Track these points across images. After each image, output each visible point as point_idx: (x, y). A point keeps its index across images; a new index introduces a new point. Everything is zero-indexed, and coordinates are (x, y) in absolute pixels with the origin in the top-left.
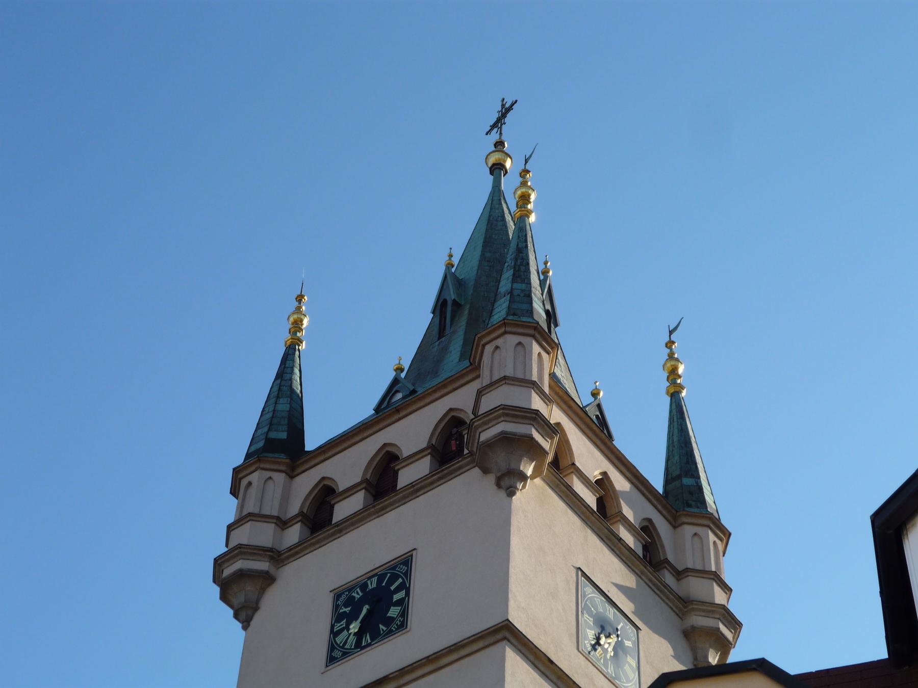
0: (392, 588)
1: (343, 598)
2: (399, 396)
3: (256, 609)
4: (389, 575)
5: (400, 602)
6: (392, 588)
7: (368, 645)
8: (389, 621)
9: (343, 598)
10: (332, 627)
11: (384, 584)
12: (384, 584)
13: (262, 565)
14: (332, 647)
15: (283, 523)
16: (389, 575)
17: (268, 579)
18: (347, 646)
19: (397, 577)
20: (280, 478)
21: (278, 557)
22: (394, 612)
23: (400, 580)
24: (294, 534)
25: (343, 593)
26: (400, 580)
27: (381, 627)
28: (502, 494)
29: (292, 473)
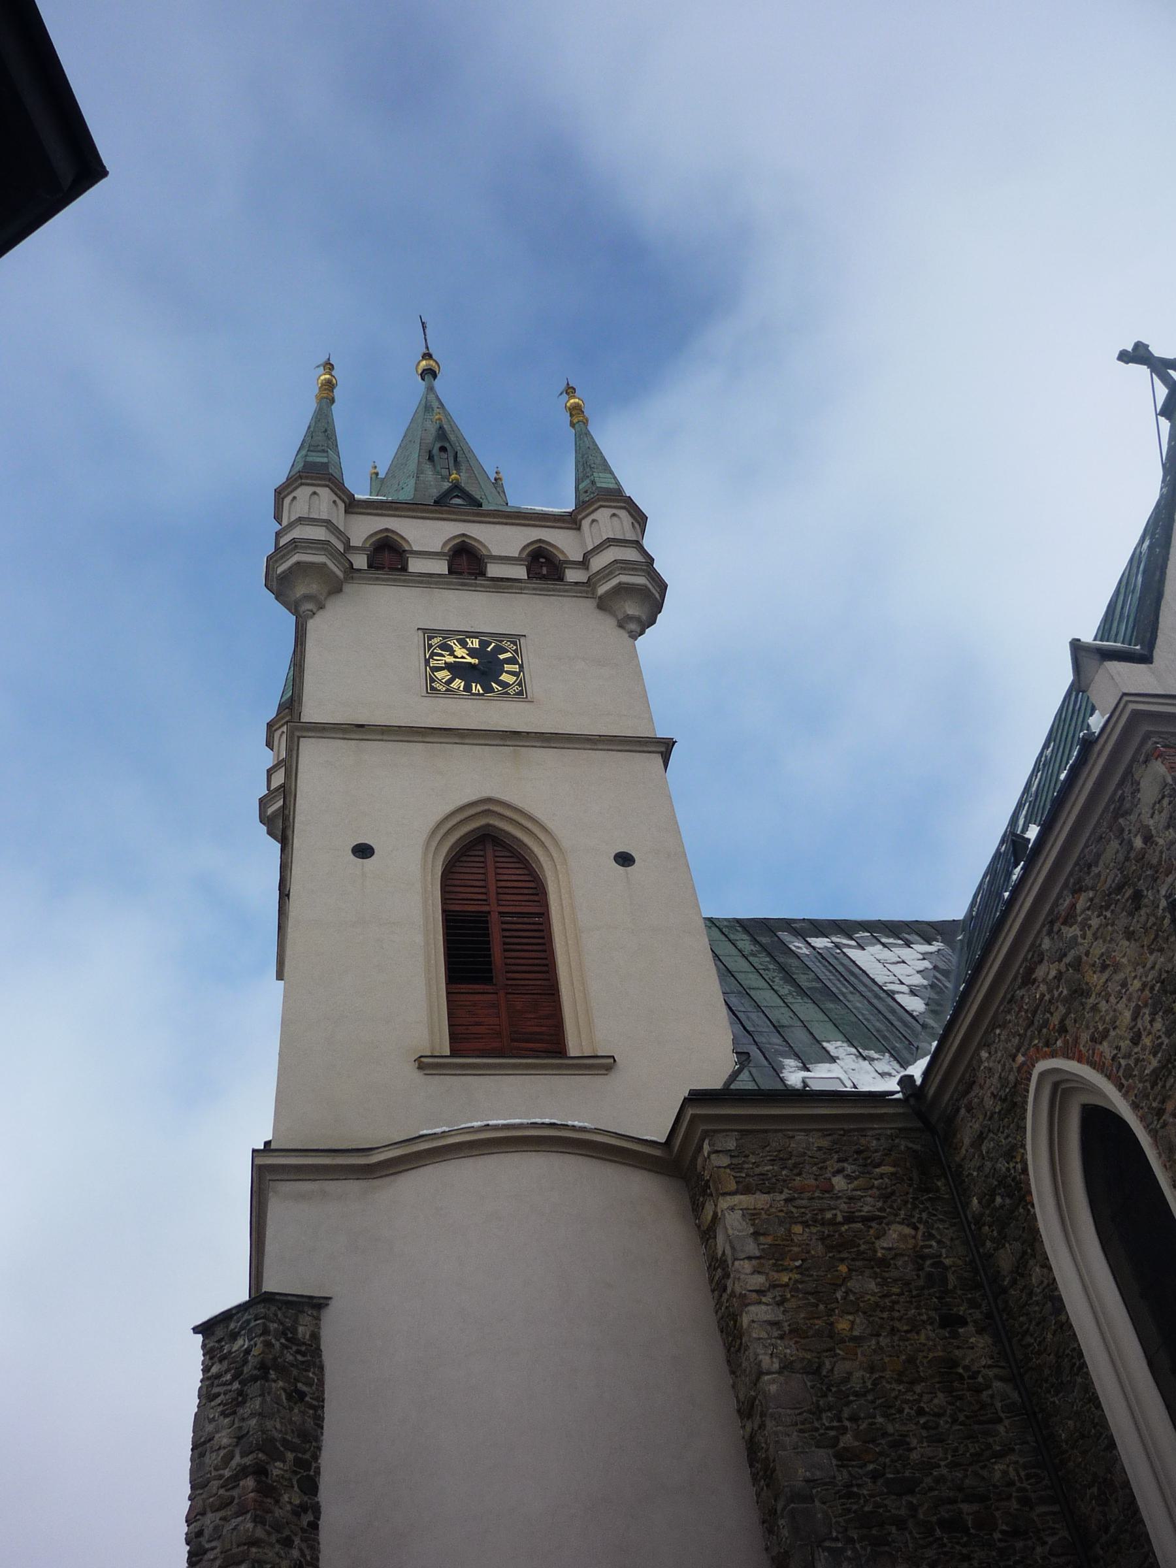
0: (502, 657)
3: (321, 607)
4: (493, 644)
6: (502, 657)
7: (482, 695)
8: (505, 685)
9: (434, 641)
10: (427, 662)
11: (489, 649)
12: (489, 649)
16: (493, 644)
23: (508, 655)
24: (360, 561)
25: (436, 637)
27: (494, 685)
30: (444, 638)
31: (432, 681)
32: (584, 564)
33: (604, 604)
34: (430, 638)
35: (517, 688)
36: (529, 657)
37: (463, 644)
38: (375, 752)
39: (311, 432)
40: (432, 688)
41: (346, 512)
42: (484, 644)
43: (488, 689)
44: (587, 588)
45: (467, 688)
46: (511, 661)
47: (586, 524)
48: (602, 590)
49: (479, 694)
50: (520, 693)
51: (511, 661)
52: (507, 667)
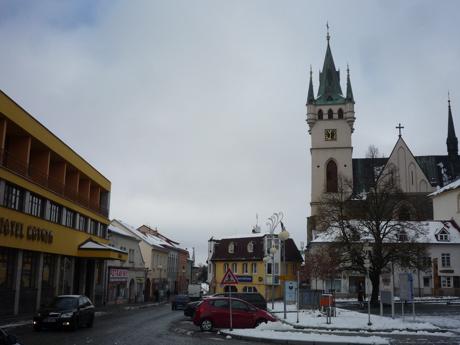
0: (334, 133)
1: (326, 131)
3: (313, 127)
5: (335, 136)
6: (334, 133)
8: (334, 138)
9: (326, 131)
14: (326, 138)
17: (314, 123)
20: (314, 106)
21: (316, 120)
22: (334, 137)
23: (335, 133)
24: (317, 117)
26: (335, 133)
29: (316, 105)
33: (347, 122)
34: (326, 131)
35: (335, 139)
36: (337, 133)
37: (329, 131)
38: (319, 150)
39: (309, 97)
40: (326, 140)
42: (332, 131)
43: (332, 139)
46: (335, 134)
47: (346, 105)
48: (348, 120)
51: (335, 134)
52: (335, 135)
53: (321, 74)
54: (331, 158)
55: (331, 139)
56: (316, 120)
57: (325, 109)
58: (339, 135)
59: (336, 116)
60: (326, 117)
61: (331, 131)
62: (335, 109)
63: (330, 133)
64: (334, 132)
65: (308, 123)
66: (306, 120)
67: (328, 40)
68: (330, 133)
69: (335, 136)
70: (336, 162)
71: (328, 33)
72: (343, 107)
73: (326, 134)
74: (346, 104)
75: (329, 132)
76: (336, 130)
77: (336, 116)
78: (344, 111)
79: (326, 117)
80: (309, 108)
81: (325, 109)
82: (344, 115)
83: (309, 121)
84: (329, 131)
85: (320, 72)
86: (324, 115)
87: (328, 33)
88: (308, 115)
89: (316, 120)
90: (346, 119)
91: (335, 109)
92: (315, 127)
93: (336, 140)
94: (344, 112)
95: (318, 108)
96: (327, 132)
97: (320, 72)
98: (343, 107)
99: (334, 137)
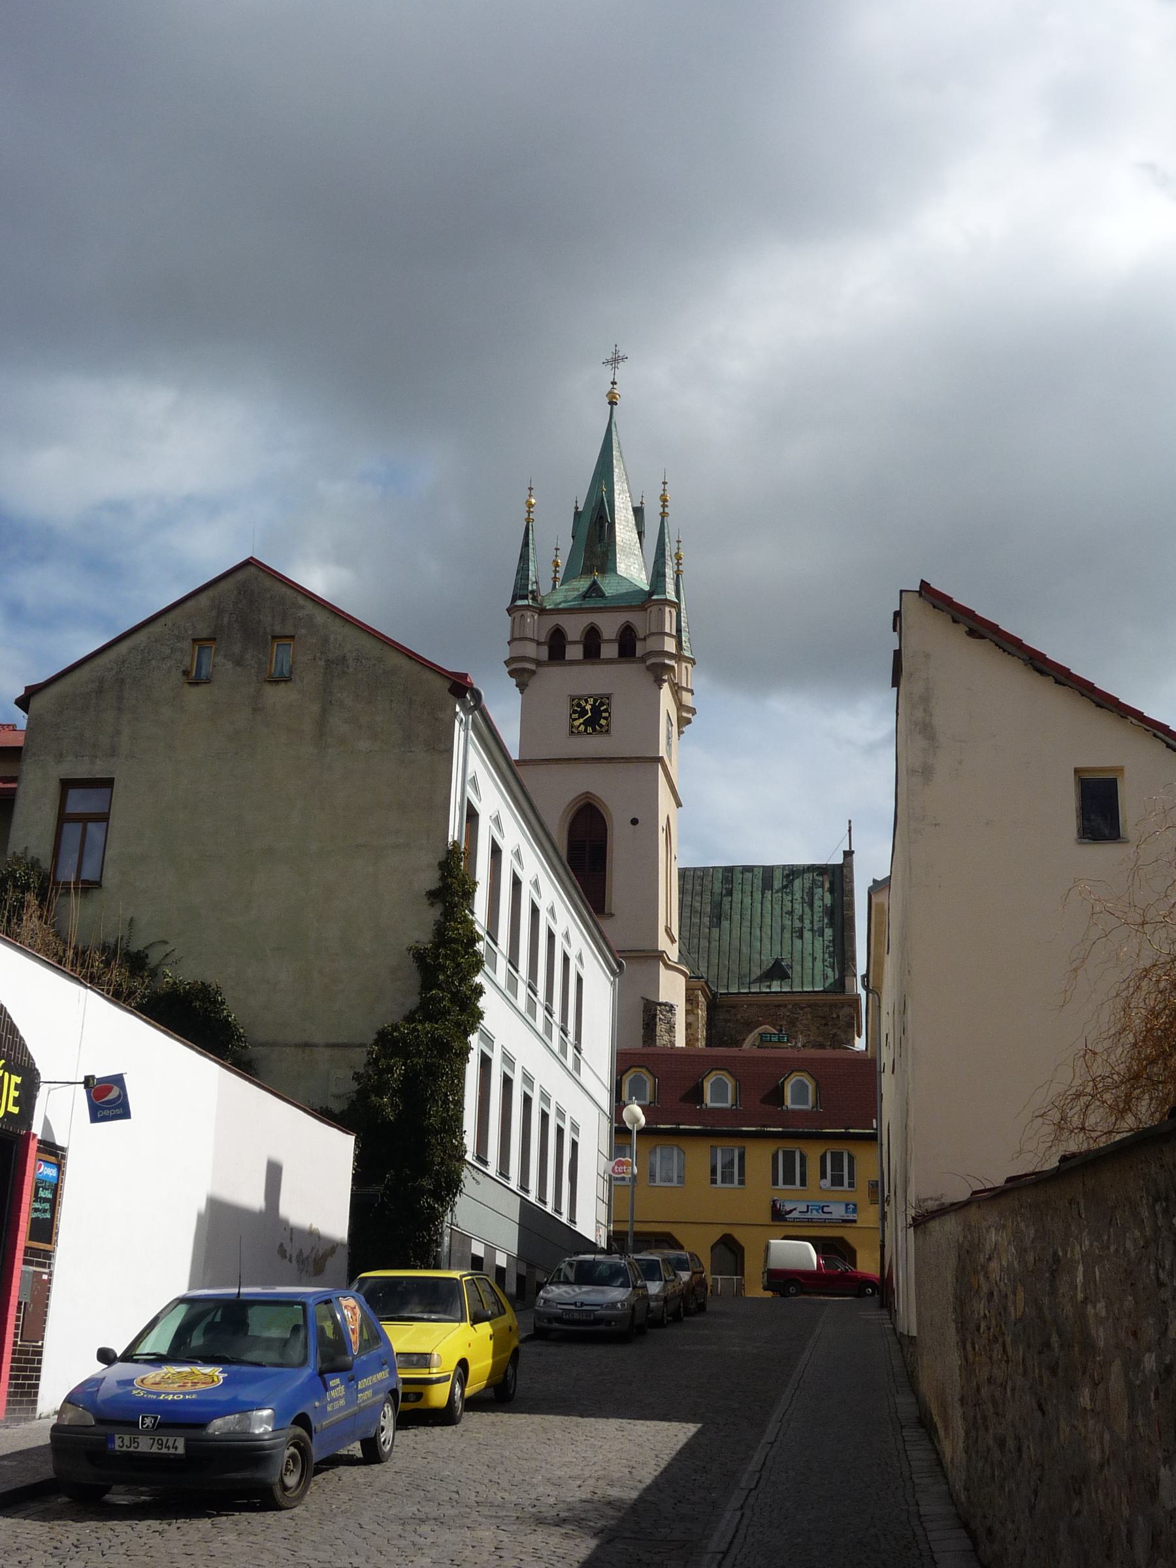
0: (602, 709)
2: (594, 595)
5: (606, 718)
6: (602, 709)
7: (590, 734)
8: (601, 726)
10: (571, 715)
13: (532, 667)
15: (539, 643)
17: (533, 672)
18: (580, 729)
19: (604, 705)
23: (605, 707)
24: (544, 653)
26: (605, 707)
28: (656, 687)
30: (579, 699)
31: (572, 727)
32: (644, 639)
33: (648, 668)
34: (573, 700)
36: (614, 709)
37: (587, 702)
40: (572, 732)
41: (539, 615)
42: (595, 701)
43: (594, 730)
44: (643, 660)
45: (586, 730)
46: (606, 711)
47: (649, 610)
48: (649, 662)
49: (590, 734)
50: (607, 731)
51: (606, 711)
52: (604, 715)
53: (577, 515)
54: (588, 793)
55: (590, 730)
56: (540, 662)
57: (574, 628)
58: (619, 715)
59: (609, 651)
60: (574, 652)
61: (591, 701)
62: (610, 626)
63: (588, 707)
64: (602, 704)
65: (512, 673)
66: (507, 663)
67: (612, 403)
68: (588, 707)
69: (606, 718)
70: (595, 801)
71: (614, 383)
72: (635, 618)
73: (575, 712)
74: (646, 610)
75: (584, 704)
76: (608, 698)
77: (609, 651)
78: (641, 634)
79: (574, 652)
80: (517, 620)
81: (574, 628)
82: (640, 649)
83: (514, 666)
84: (587, 702)
85: (577, 508)
86: (572, 646)
87: (614, 383)
88: (515, 643)
89: (539, 663)
90: (643, 660)
91: (610, 626)
92: (534, 684)
93: (607, 731)
94: (641, 634)
95: (551, 622)
96: (579, 705)
97: (577, 508)
98: (635, 618)
99: (603, 722)
